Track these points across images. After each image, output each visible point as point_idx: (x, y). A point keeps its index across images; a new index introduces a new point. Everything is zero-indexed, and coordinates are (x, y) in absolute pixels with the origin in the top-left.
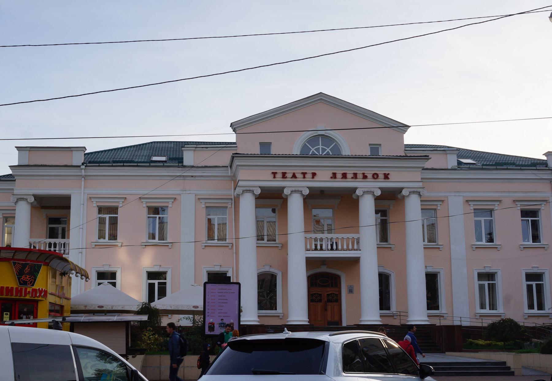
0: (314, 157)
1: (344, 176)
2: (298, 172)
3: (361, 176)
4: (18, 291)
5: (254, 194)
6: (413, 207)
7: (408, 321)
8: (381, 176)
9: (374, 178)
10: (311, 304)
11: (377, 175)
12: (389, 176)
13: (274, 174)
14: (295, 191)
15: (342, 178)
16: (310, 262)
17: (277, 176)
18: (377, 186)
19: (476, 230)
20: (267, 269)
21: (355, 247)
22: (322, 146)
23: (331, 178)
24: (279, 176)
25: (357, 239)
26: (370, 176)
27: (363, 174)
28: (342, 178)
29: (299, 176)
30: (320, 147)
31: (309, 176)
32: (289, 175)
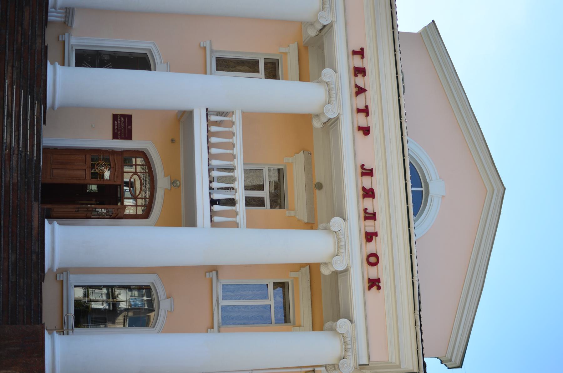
2: (370, 99)
3: (371, 230)
8: (373, 273)
10: (88, 157)
12: (375, 288)
13: (360, 53)
15: (364, 189)
16: (185, 118)
17: (357, 58)
23: (363, 165)
24: (358, 62)
26: (371, 247)
27: (376, 234)
28: (364, 189)
31: (362, 120)
32: (360, 81)
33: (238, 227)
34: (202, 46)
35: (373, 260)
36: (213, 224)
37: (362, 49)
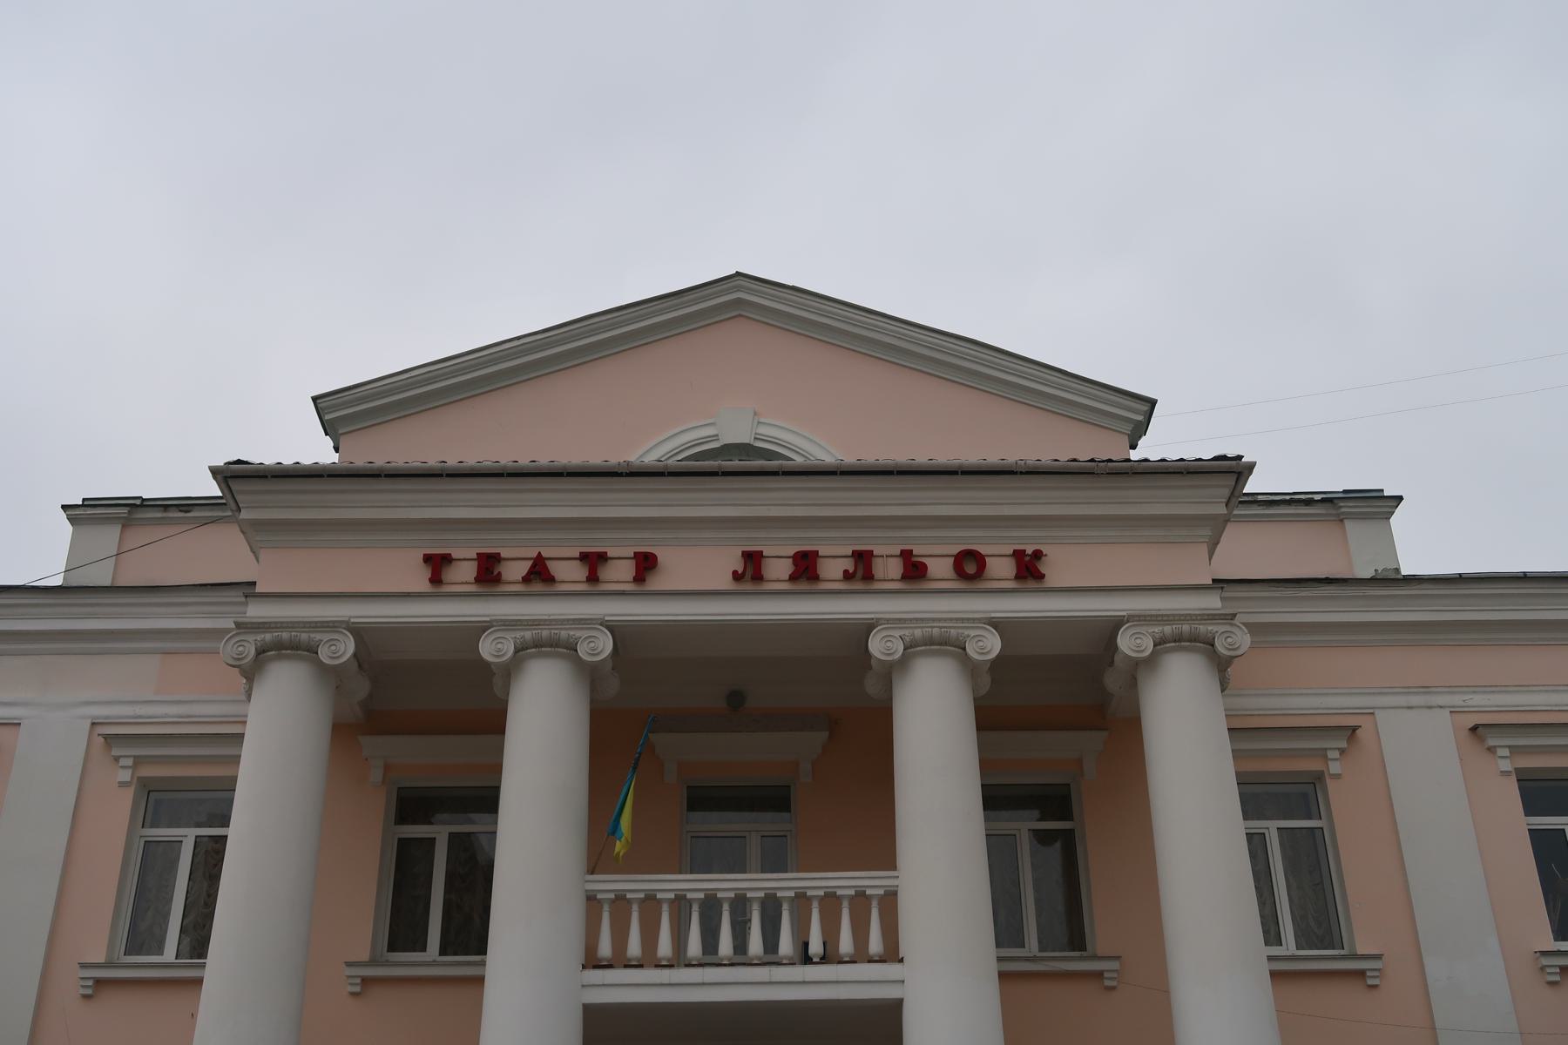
1: (806, 567)
3: (895, 568)
5: (320, 665)
8: (1001, 568)
9: (960, 572)
11: (979, 559)
13: (437, 564)
14: (538, 644)
15: (793, 578)
21: (875, 945)
23: (737, 577)
24: (464, 572)
25: (882, 899)
26: (940, 568)
27: (906, 555)
29: (569, 572)
31: (620, 572)
32: (514, 571)
33: (895, 894)
34: (357, 989)
37: (428, 559)
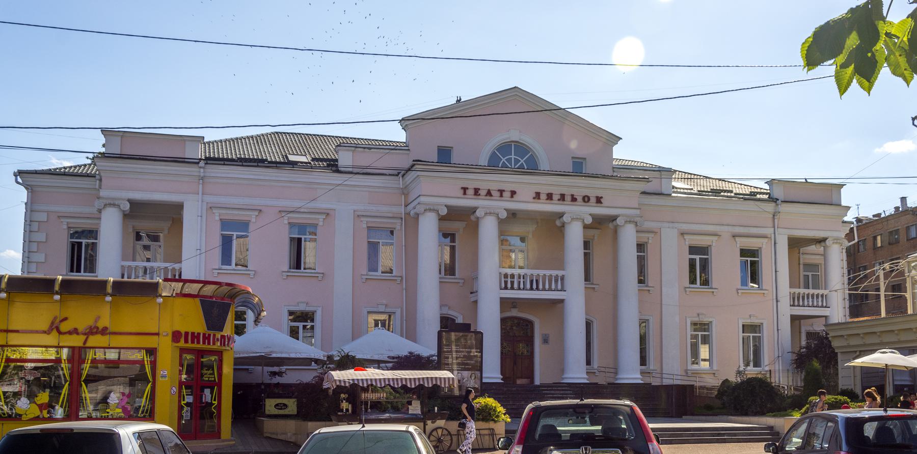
0: (505, 170)
2: (494, 187)
4: (206, 338)
6: (628, 238)
7: (617, 379)
8: (593, 200)
9: (584, 201)
13: (465, 190)
18: (587, 211)
19: (690, 272)
20: (446, 311)
22: (515, 158)
24: (470, 192)
26: (580, 199)
27: (572, 195)
29: (496, 194)
30: (513, 157)
31: (507, 195)
35: (586, 199)
36: (563, 290)
